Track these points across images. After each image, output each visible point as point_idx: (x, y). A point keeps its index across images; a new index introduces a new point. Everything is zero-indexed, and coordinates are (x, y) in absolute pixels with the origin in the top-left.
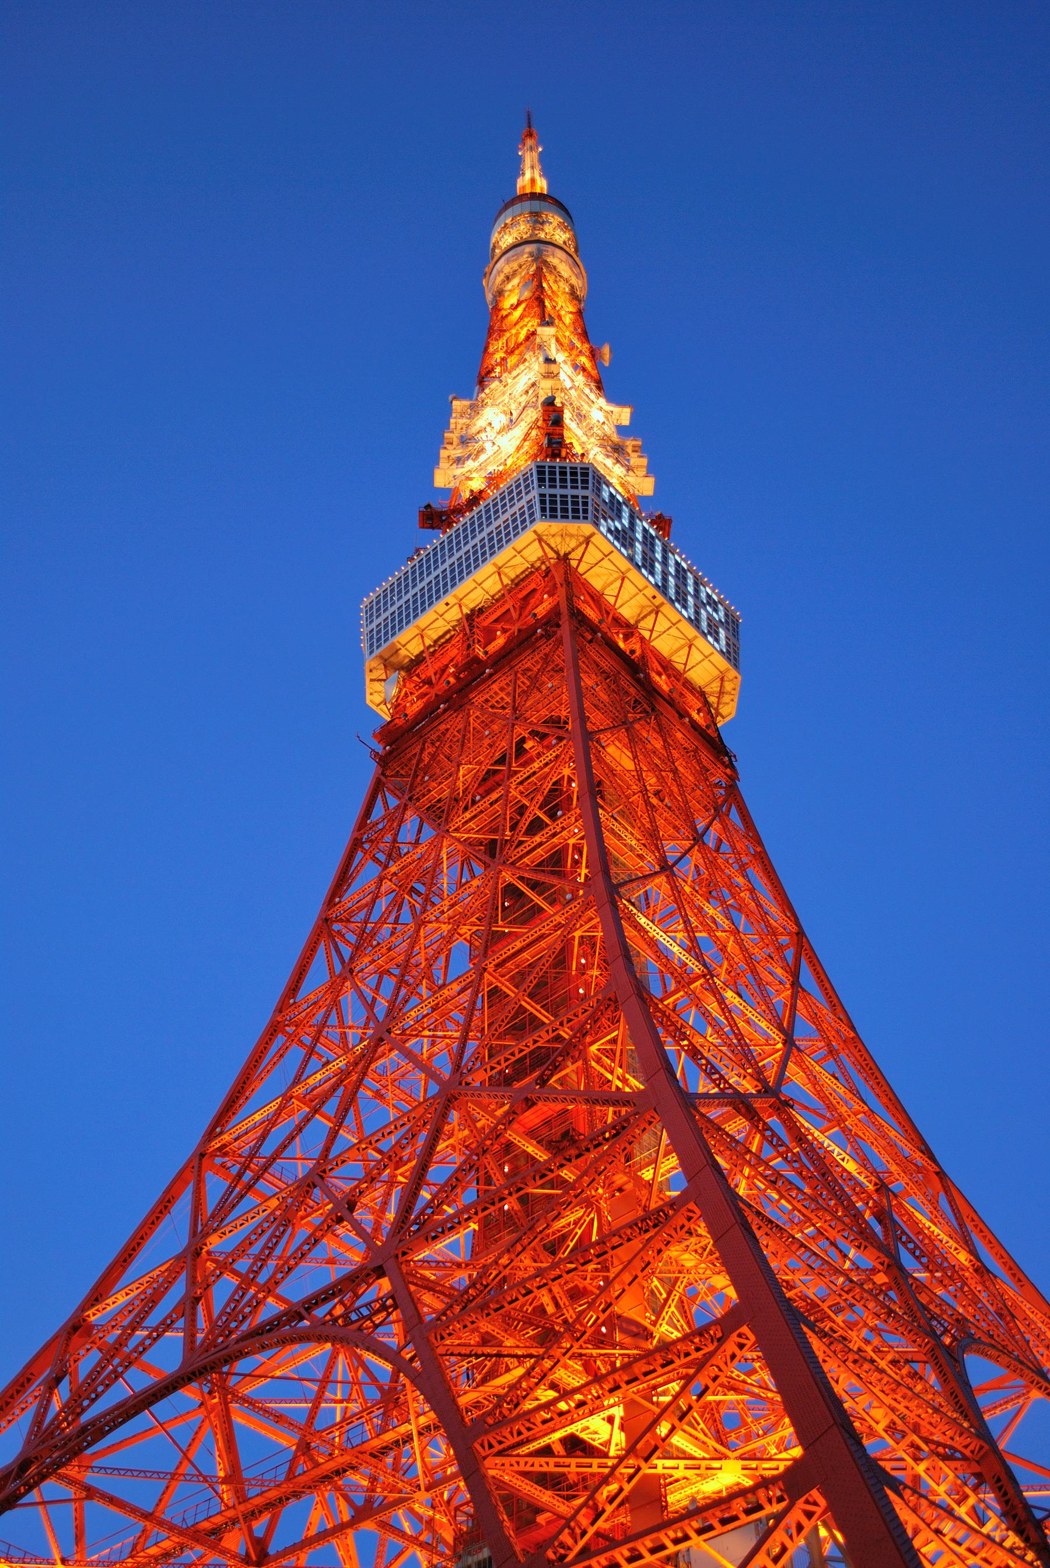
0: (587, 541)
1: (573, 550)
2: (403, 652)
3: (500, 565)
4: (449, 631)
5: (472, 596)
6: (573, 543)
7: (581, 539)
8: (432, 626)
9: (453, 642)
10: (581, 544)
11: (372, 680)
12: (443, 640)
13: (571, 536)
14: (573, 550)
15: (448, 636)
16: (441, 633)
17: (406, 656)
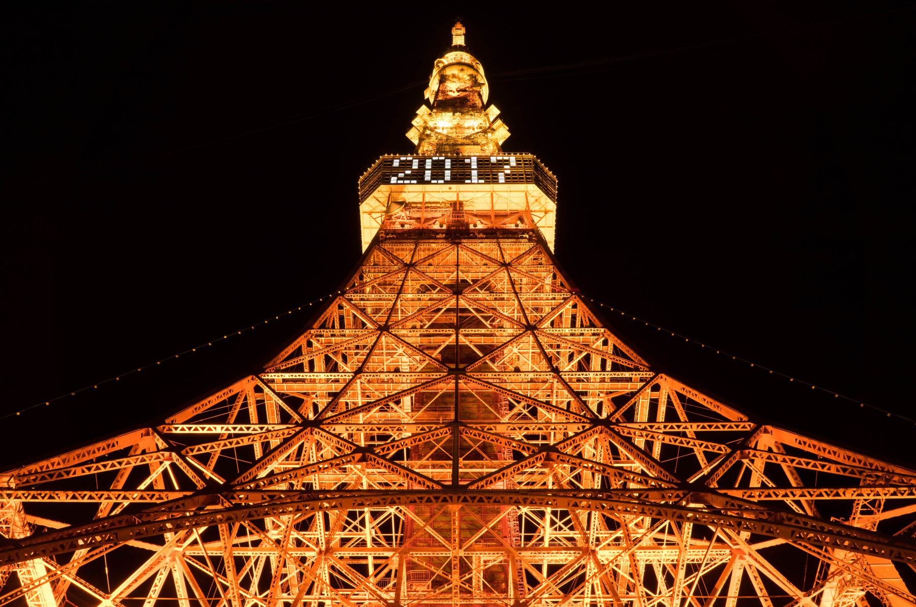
0: (546, 212)
1: (535, 211)
2: (403, 195)
3: (495, 190)
4: (439, 203)
5: (465, 194)
6: (537, 208)
7: (543, 209)
8: (430, 193)
9: (442, 209)
10: (541, 211)
11: (375, 197)
12: (429, 205)
13: (540, 203)
14: (535, 211)
15: (433, 205)
16: (432, 200)
17: (403, 198)
